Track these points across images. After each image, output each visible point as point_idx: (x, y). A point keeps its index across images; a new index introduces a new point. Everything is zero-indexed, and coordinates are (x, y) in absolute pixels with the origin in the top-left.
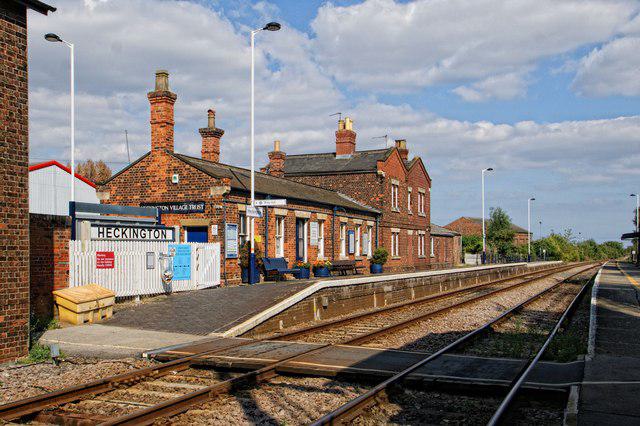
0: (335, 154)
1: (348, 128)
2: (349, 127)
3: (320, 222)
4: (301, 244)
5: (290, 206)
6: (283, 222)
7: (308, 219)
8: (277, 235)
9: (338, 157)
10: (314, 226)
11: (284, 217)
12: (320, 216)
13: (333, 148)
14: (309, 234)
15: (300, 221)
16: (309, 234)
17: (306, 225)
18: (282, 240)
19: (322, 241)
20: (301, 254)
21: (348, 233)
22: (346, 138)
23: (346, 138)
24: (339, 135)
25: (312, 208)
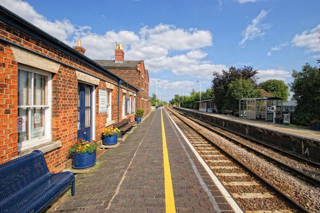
0: (114, 61)
1: (121, 48)
2: (121, 48)
3: (109, 91)
4: (87, 113)
5: (64, 61)
6: (50, 83)
7: (96, 86)
8: (38, 106)
9: (116, 62)
10: (103, 94)
11: (53, 74)
12: (109, 85)
13: (114, 59)
14: (97, 102)
15: (83, 87)
16: (97, 102)
17: (94, 93)
18: (48, 113)
19: (110, 107)
20: (87, 124)
21: (127, 100)
22: (120, 53)
23: (120, 53)
24: (117, 51)
25: (102, 77)
